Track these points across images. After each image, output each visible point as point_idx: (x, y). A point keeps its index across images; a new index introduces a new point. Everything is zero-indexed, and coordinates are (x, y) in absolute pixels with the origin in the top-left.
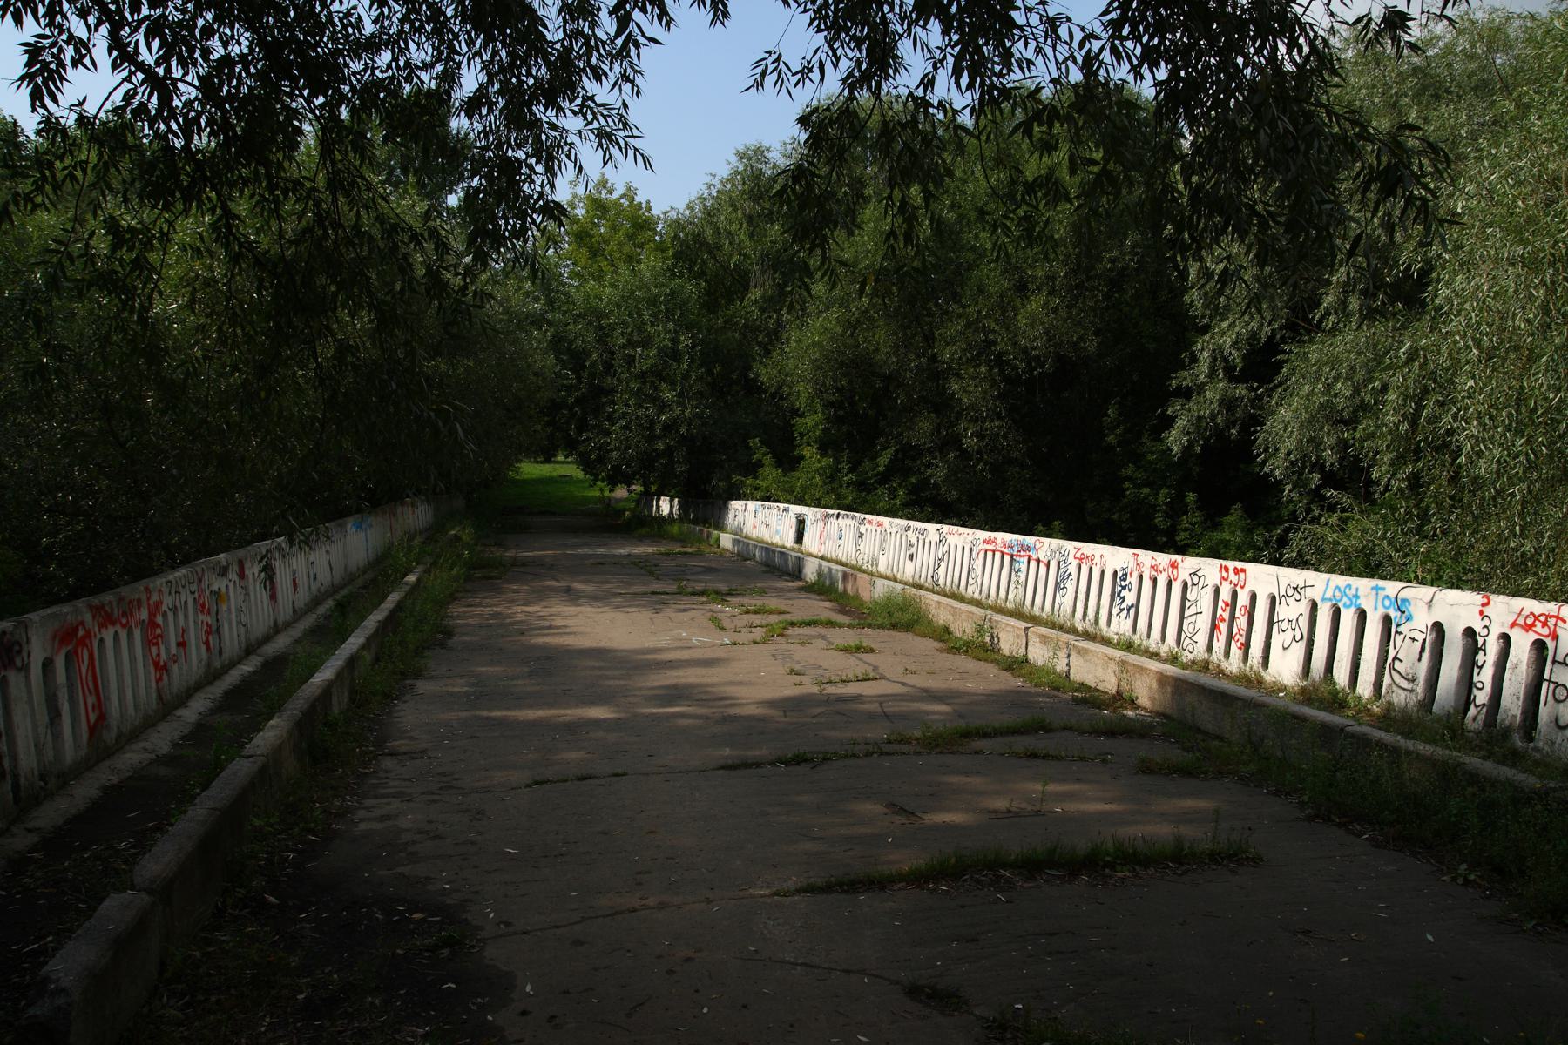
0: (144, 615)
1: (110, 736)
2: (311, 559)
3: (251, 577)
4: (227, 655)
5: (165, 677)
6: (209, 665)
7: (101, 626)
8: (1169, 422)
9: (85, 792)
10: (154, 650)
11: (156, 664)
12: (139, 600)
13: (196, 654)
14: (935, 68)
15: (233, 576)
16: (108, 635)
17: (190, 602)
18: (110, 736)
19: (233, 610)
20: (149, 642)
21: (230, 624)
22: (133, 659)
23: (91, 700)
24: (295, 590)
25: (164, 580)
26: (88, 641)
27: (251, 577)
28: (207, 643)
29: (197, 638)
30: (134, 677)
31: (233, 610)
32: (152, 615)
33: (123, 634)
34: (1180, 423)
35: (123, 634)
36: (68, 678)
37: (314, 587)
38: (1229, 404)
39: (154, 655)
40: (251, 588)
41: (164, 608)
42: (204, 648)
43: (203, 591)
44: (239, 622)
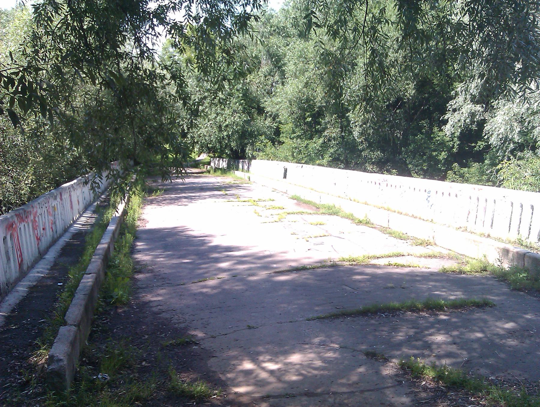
0: (32, 217)
1: (25, 267)
2: (83, 191)
3: (64, 200)
4: (58, 232)
5: (40, 243)
6: (53, 237)
7: (20, 222)
8: (445, 122)
9: (22, 289)
10: (36, 231)
11: (37, 238)
12: (30, 211)
13: (49, 232)
14: (276, 376)
15: (58, 199)
16: (22, 226)
17: (46, 211)
18: (25, 267)
19: (59, 214)
20: (34, 229)
21: (59, 219)
22: (30, 236)
23: (19, 253)
24: (79, 204)
25: (37, 203)
26: (16, 229)
27: (64, 200)
28: (52, 228)
29: (49, 226)
30: (31, 243)
31: (59, 214)
32: (35, 217)
33: (26, 225)
34: (450, 123)
35: (26, 225)
36: (12, 244)
37: (85, 202)
38: (472, 115)
39: (36, 233)
40: (65, 204)
41: (38, 214)
42: (51, 230)
43: (50, 206)
44: (62, 218)
